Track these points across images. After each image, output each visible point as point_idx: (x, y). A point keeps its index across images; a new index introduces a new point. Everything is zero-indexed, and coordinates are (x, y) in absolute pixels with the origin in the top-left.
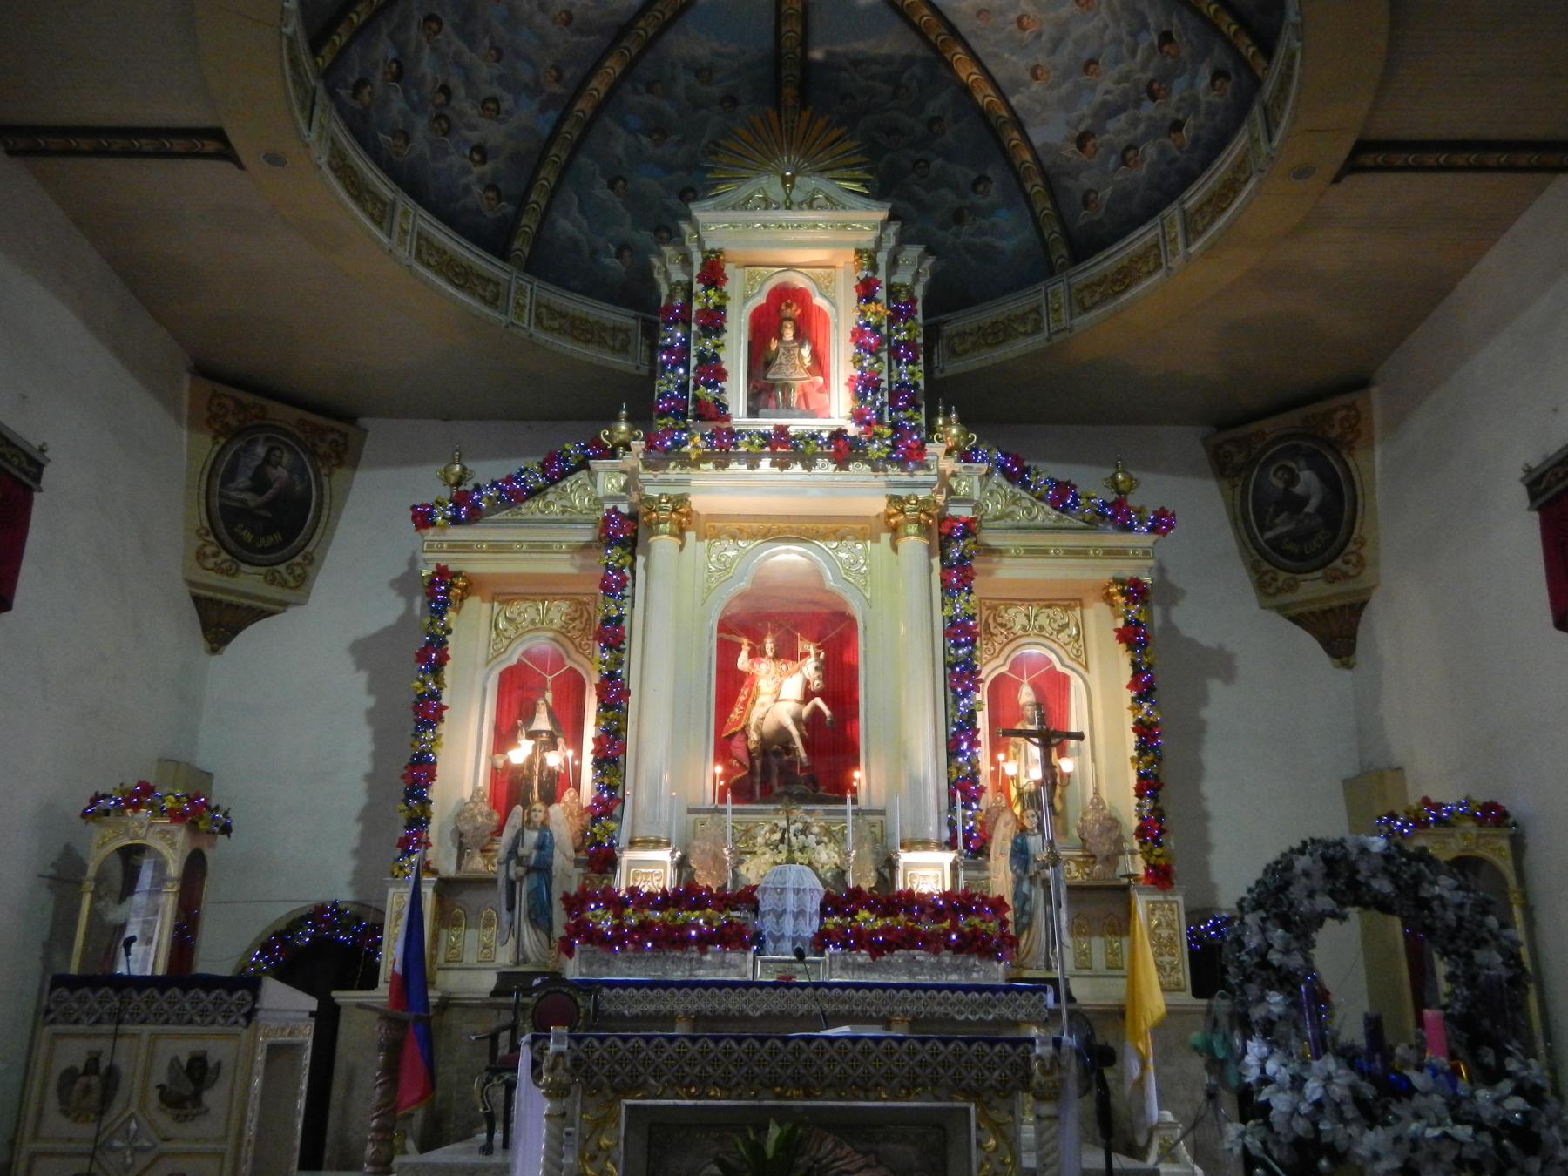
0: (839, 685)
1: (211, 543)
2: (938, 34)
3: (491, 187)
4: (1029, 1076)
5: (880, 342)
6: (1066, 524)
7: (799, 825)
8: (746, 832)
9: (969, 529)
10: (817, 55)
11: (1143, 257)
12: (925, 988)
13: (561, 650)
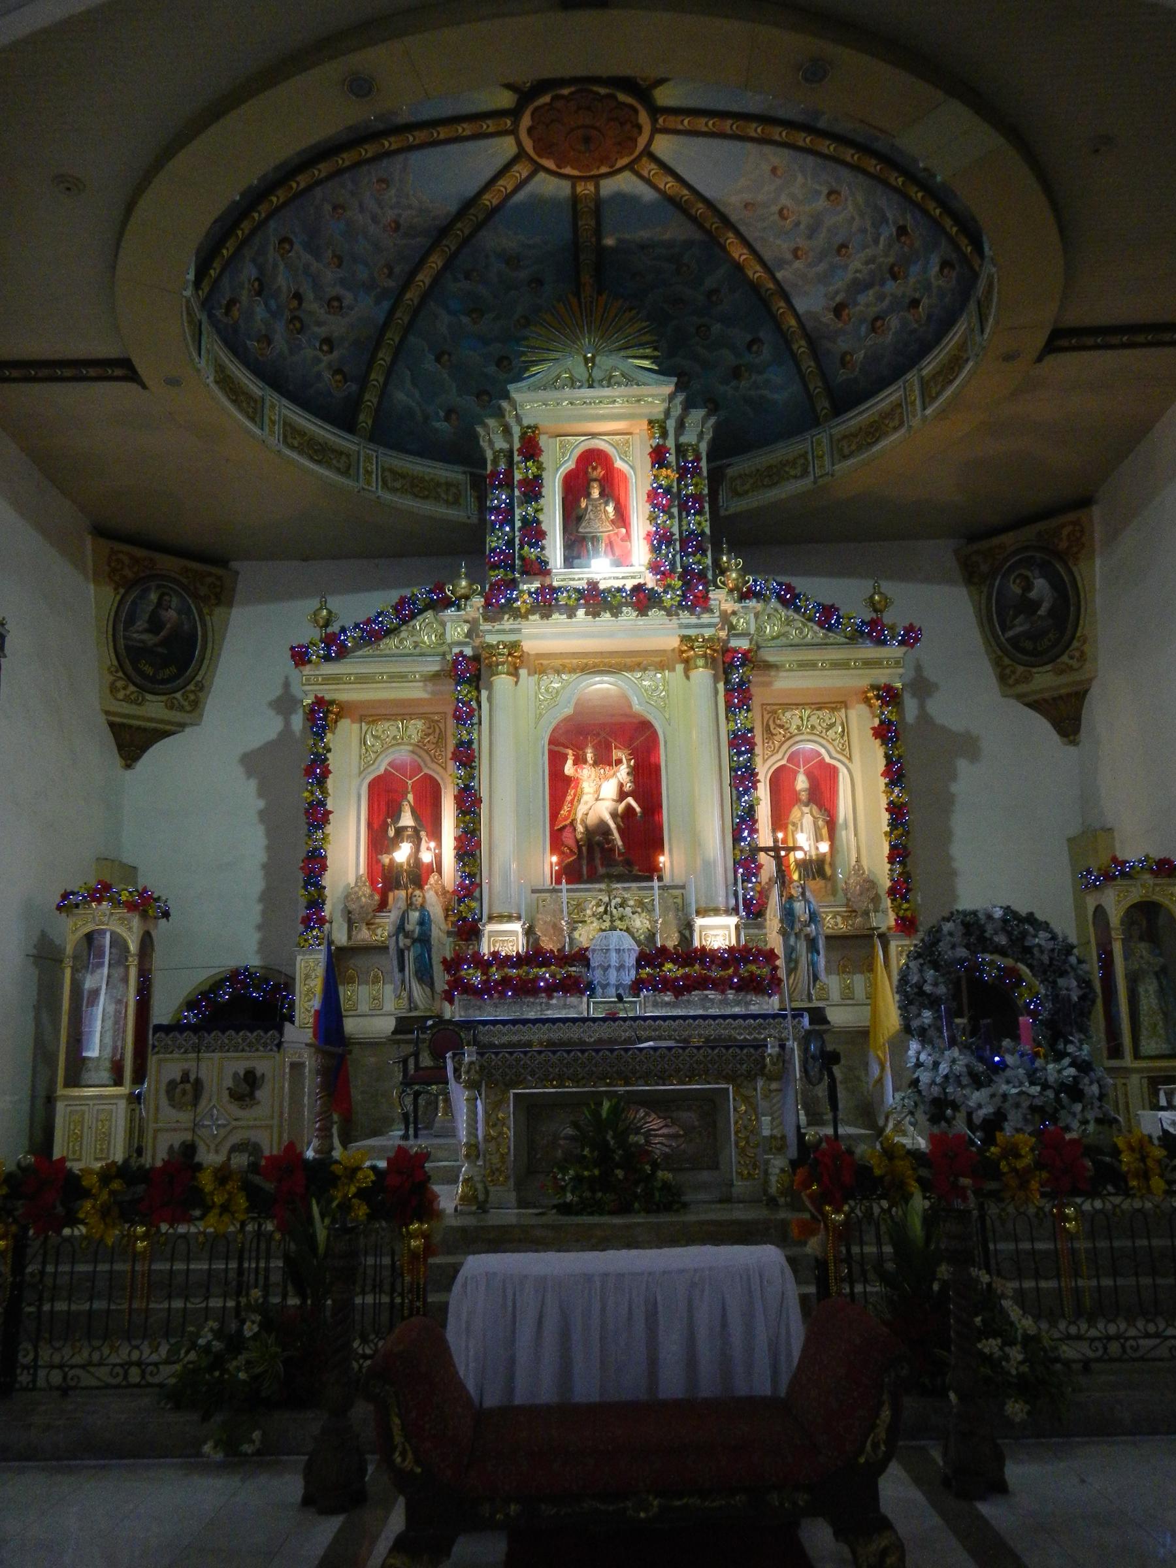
0: (646, 783)
1: (121, 678)
2: (713, 223)
3: (338, 371)
4: (764, 1066)
5: (671, 501)
6: (831, 640)
7: (618, 900)
8: (578, 905)
9: (747, 658)
10: (609, 242)
11: (888, 415)
12: (714, 1017)
13: (419, 760)
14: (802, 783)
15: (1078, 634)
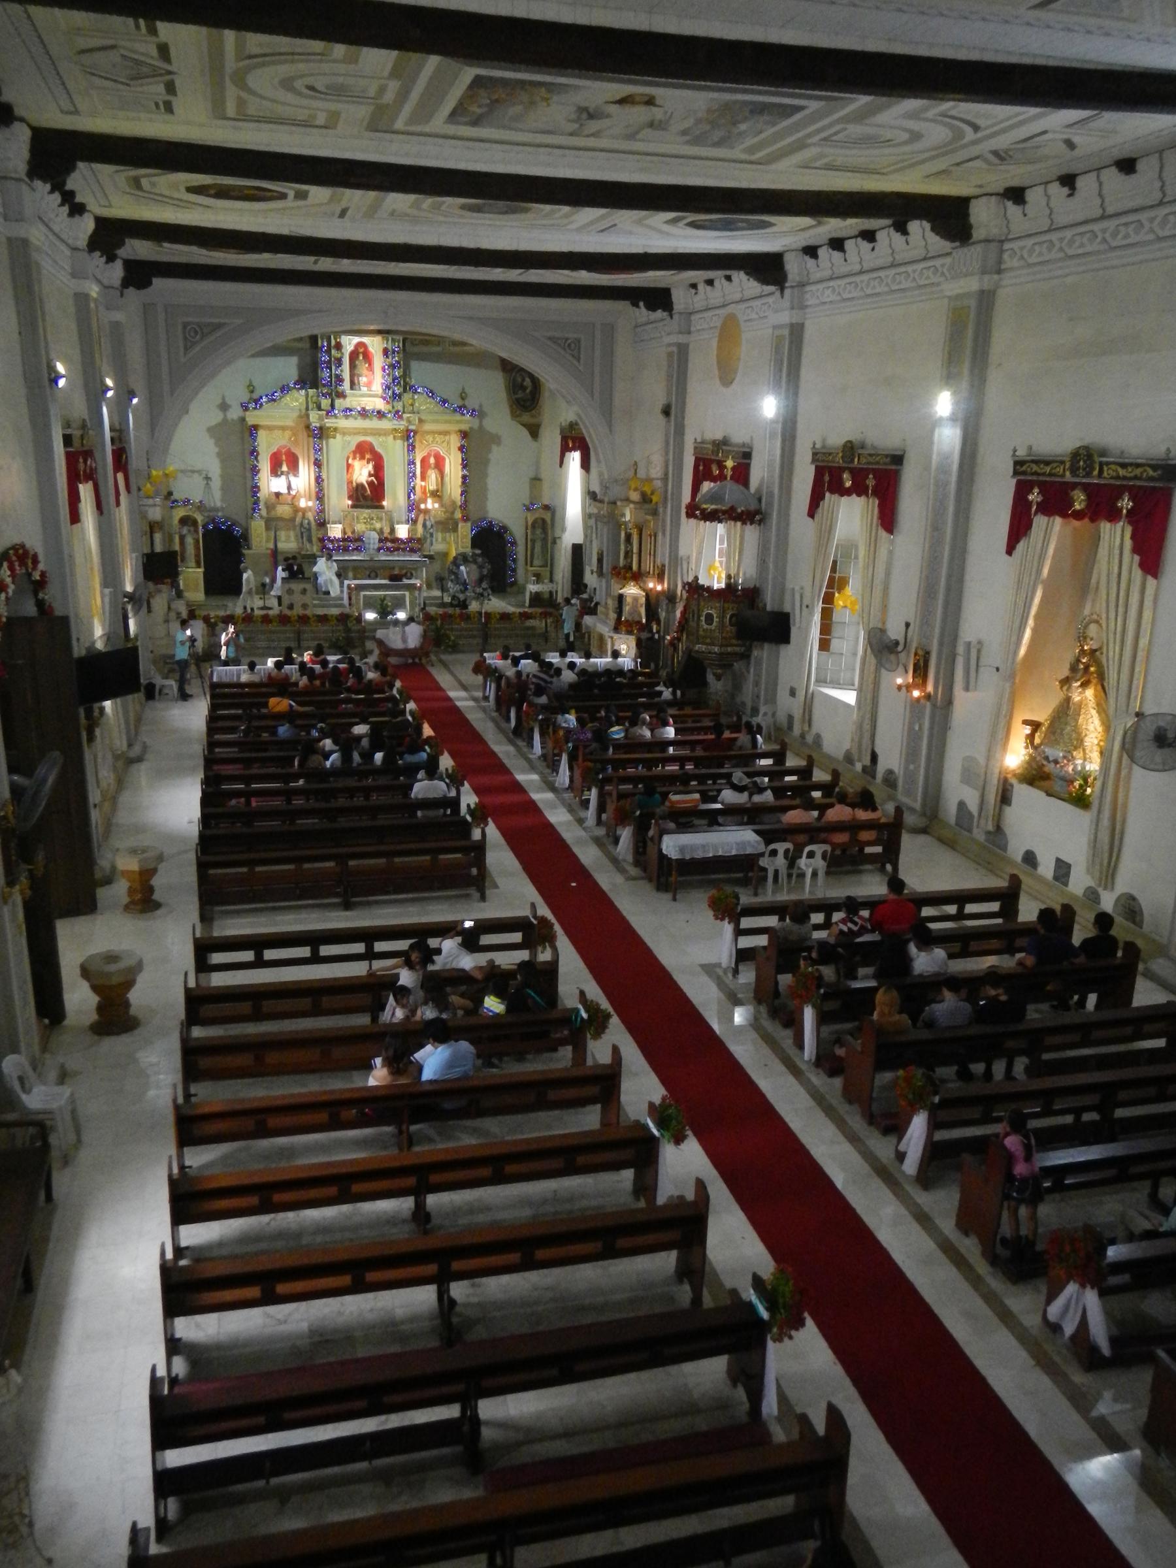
14: (432, 460)
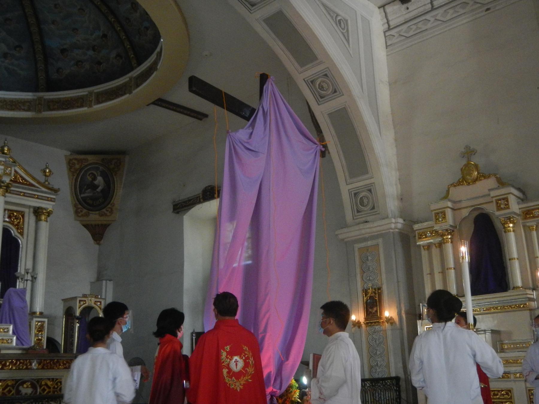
15: (112, 202)
